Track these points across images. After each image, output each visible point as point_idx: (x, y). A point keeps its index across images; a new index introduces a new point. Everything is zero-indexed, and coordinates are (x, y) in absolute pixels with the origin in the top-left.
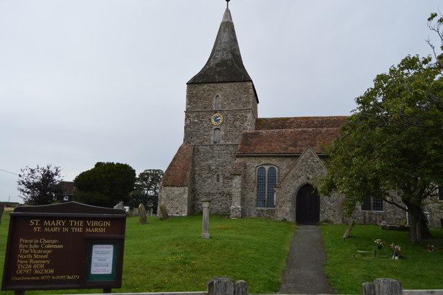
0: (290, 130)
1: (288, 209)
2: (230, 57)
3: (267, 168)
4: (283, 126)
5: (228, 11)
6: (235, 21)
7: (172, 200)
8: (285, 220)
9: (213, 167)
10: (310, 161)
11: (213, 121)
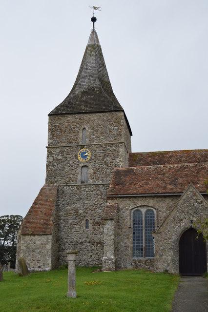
0: (168, 166)
1: (170, 258)
2: (98, 83)
3: (144, 210)
4: (161, 162)
5: (94, 33)
6: (102, 44)
7: (33, 251)
8: (167, 271)
9: (81, 212)
10: (193, 201)
11: (79, 158)
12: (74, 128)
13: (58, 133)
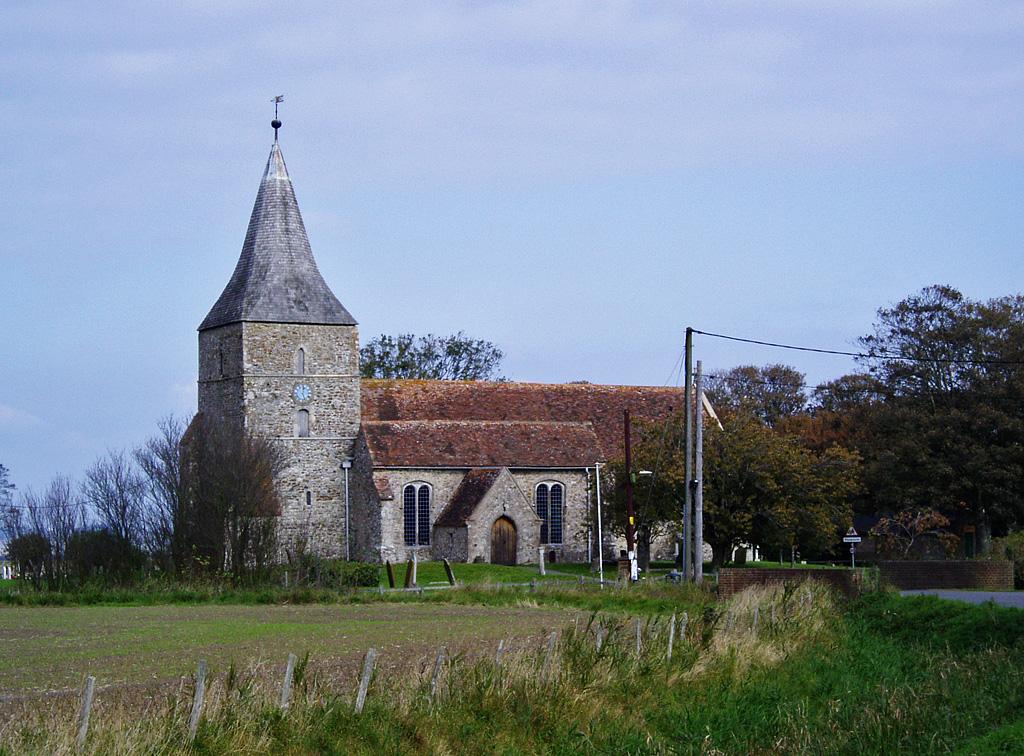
3: (417, 487)
9: (299, 479)
12: (284, 346)
13: (259, 352)
